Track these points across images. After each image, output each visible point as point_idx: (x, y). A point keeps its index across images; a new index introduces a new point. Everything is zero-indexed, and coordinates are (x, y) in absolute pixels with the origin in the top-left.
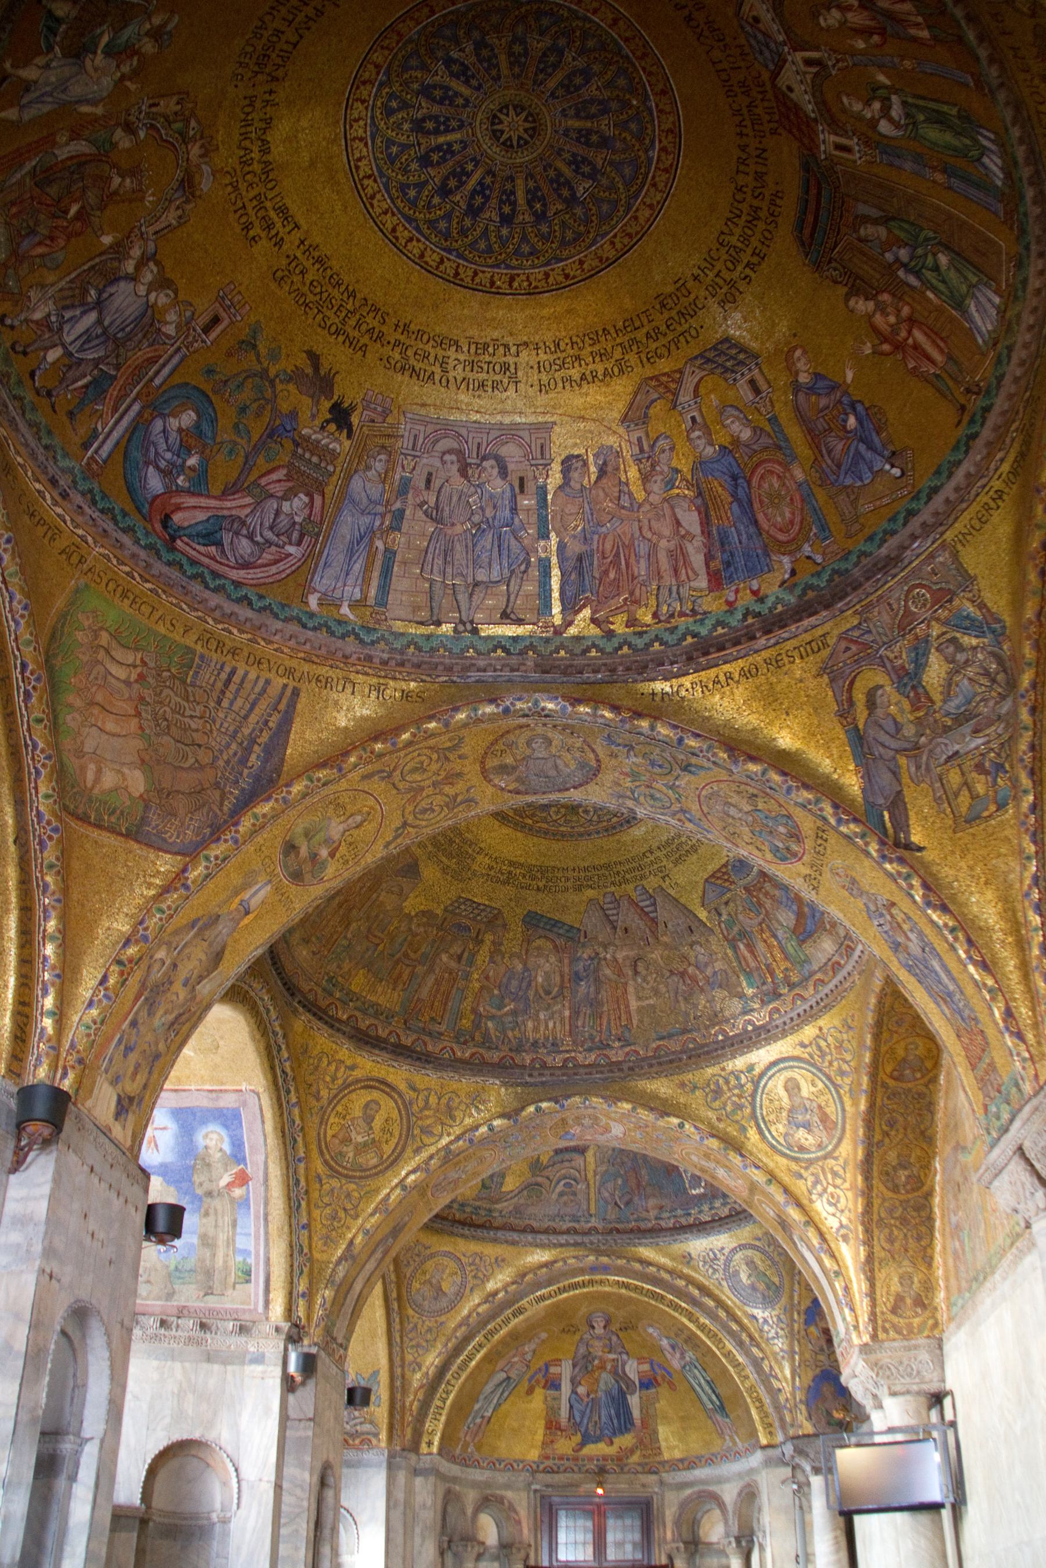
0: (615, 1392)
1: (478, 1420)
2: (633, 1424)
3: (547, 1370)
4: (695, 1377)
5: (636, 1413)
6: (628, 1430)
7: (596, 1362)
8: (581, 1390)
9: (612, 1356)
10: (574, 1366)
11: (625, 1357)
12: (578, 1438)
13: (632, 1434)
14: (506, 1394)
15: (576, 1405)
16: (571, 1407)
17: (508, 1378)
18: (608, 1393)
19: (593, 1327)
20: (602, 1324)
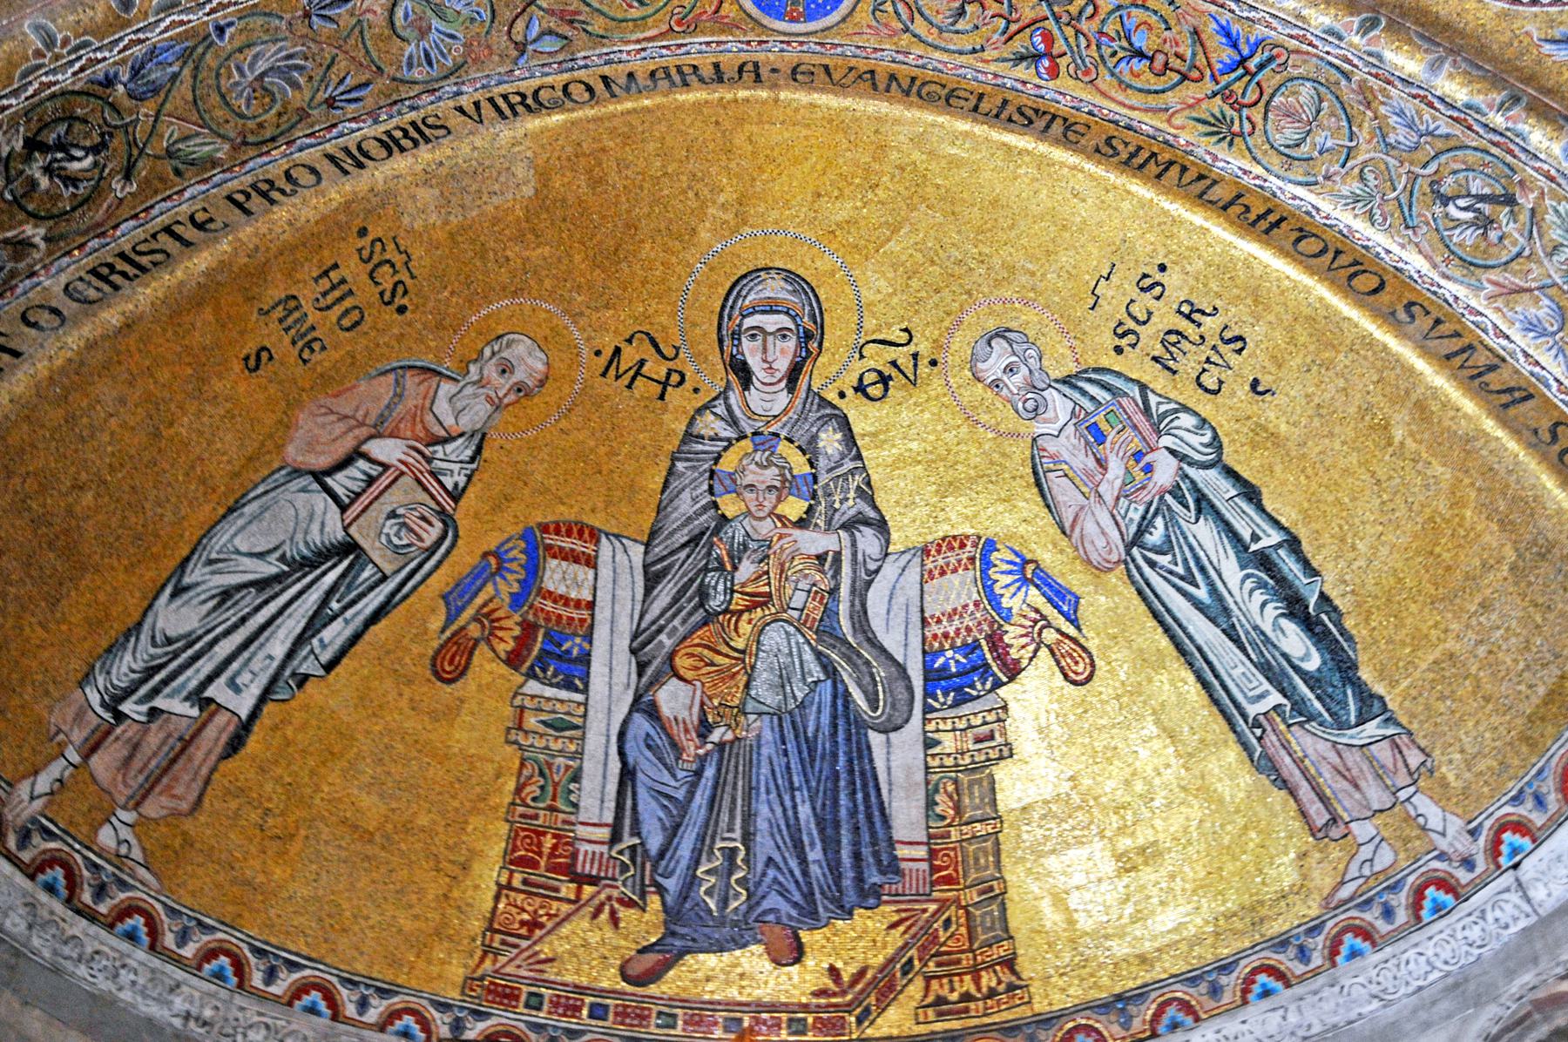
0: (818, 720)
1: (174, 704)
2: (892, 867)
3: (533, 570)
4: (1197, 570)
5: (907, 818)
6: (870, 896)
7: (746, 569)
8: (673, 699)
9: (815, 541)
10: (652, 580)
11: (868, 541)
12: (646, 923)
13: (888, 912)
14: (334, 634)
15: (649, 769)
16: (628, 774)
17: (349, 548)
18: (788, 720)
19: (743, 373)
20: (783, 354)
